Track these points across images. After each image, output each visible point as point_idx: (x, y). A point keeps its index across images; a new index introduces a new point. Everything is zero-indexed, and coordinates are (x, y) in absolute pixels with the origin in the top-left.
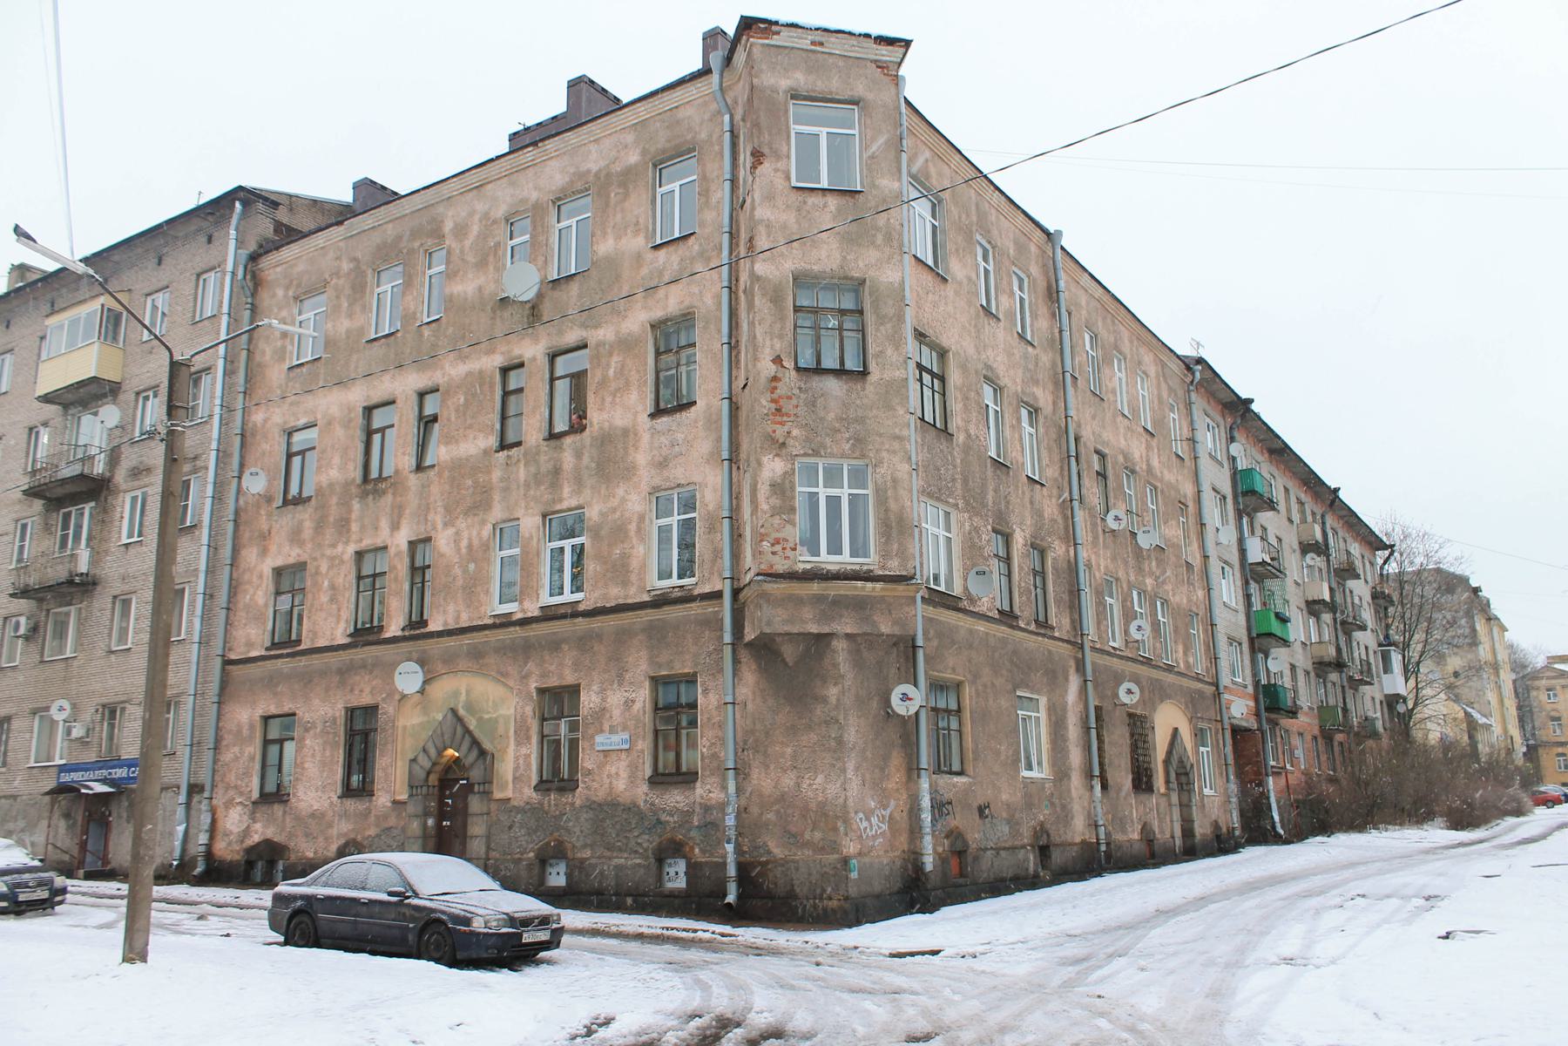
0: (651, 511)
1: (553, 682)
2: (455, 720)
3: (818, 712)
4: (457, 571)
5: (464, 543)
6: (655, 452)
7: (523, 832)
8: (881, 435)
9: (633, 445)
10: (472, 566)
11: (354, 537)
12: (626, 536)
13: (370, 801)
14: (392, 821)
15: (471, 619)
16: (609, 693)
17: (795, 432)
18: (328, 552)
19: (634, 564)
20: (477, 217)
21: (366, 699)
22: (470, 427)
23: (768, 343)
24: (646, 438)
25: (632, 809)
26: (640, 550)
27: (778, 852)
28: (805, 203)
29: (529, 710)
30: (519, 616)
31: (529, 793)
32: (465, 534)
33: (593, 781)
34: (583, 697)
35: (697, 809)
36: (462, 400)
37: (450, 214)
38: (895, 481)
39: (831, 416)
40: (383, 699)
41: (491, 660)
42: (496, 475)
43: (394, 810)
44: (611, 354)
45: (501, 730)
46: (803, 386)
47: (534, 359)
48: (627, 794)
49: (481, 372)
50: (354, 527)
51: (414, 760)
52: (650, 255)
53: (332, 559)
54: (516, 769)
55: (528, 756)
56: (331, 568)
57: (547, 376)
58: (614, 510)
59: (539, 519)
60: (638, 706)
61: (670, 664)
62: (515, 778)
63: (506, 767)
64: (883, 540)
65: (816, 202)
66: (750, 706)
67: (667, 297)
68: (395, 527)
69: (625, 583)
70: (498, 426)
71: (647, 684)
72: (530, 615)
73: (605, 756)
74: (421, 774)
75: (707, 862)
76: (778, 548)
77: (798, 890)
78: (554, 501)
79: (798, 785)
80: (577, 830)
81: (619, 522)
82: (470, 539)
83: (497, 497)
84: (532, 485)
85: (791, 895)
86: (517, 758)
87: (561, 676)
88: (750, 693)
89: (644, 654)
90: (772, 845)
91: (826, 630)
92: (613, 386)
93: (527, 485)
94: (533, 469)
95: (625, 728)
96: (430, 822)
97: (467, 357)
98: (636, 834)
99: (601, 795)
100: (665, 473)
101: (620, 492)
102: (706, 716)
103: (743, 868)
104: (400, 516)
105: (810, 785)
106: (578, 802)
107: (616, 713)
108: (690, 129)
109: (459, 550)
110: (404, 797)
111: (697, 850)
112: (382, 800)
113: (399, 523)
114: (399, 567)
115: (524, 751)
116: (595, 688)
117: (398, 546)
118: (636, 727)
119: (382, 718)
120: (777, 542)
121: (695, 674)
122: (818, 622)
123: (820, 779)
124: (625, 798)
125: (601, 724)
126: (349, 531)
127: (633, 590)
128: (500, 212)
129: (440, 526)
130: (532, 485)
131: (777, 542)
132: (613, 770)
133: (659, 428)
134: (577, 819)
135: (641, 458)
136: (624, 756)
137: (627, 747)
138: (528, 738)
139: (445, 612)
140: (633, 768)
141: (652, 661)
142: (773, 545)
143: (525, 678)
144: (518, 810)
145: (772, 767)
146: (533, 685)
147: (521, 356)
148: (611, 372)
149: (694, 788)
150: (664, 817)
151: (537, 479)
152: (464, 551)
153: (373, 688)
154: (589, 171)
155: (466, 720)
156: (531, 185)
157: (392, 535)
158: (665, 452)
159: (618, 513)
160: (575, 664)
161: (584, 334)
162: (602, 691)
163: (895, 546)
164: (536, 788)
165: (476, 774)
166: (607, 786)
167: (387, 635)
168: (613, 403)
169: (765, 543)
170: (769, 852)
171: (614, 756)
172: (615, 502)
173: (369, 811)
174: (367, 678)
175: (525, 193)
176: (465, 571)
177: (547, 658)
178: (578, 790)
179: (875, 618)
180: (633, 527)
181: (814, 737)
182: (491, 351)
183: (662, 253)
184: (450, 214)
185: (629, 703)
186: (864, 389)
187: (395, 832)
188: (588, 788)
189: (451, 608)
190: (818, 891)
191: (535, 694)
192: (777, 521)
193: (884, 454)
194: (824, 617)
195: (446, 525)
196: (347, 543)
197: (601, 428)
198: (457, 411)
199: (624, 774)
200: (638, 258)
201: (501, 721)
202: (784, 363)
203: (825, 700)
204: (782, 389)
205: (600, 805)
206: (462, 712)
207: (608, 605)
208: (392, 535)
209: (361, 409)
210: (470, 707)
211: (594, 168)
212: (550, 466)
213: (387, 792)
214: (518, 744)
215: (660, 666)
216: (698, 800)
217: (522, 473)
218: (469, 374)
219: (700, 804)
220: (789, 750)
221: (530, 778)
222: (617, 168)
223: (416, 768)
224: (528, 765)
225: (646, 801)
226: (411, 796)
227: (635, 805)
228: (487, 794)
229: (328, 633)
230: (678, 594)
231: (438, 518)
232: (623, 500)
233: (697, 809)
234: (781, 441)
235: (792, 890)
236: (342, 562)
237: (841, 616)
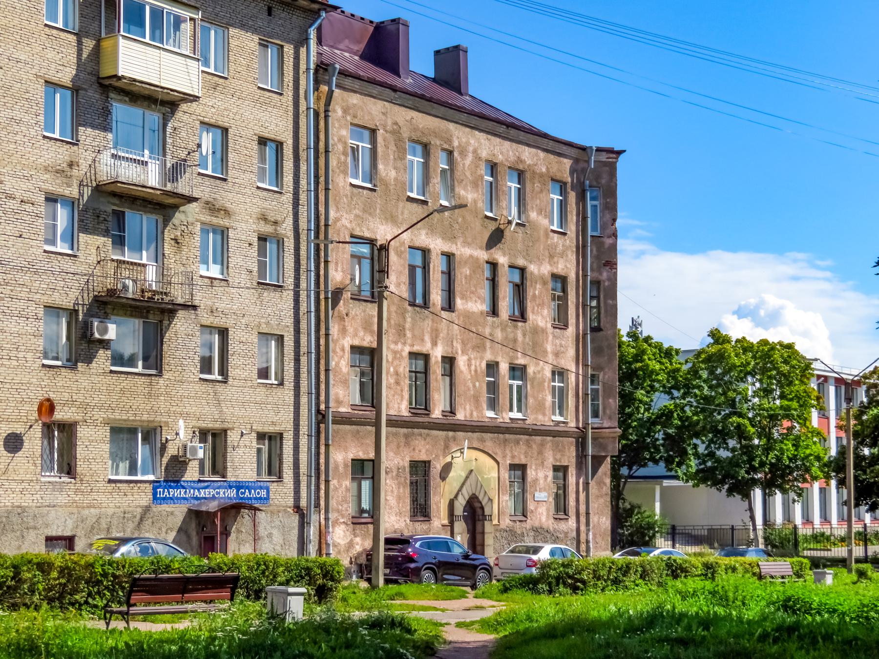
1: (517, 461)
5: (473, 368)
11: (409, 341)
21: (423, 457)
43: (443, 529)
58: (539, 372)
68: (434, 344)
87: (520, 459)
89: (551, 452)
95: (545, 490)
99: (537, 524)
106: (528, 527)
113: (436, 342)
117: (436, 357)
124: (545, 526)
126: (405, 335)
129: (460, 352)
136: (544, 503)
146: (508, 462)
152: (473, 372)
157: (432, 349)
158: (558, 348)
176: (474, 386)
185: (546, 477)
199: (545, 513)
201: (492, 479)
208: (432, 349)
218: (471, 256)
229: (396, 406)
231: (458, 346)
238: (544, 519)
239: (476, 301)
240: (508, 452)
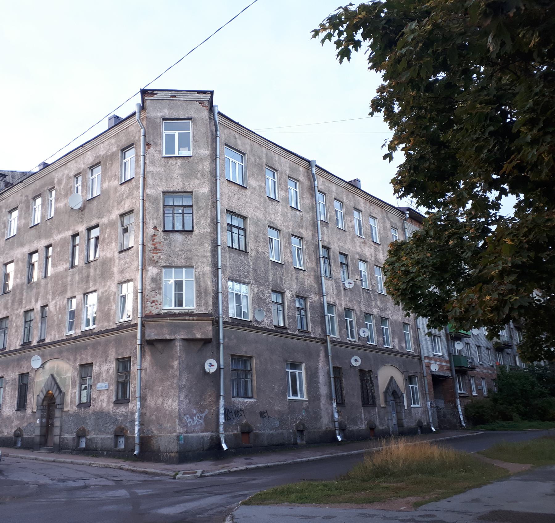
0: (118, 291)
1: (84, 362)
2: (52, 379)
3: (170, 372)
4: (55, 318)
5: (58, 307)
6: (120, 267)
7: (72, 424)
8: (198, 256)
9: (113, 265)
10: (60, 316)
11: (24, 306)
12: (110, 302)
13: (25, 412)
14: (32, 420)
15: (59, 337)
16: (102, 366)
17: (162, 257)
18: (16, 312)
19: (112, 312)
20: (65, 176)
21: (25, 371)
22: (61, 260)
23: (151, 221)
24: (117, 261)
25: (107, 414)
26: (114, 307)
27: (156, 432)
28: (168, 163)
29: (76, 374)
30: (74, 335)
31: (75, 408)
32: (58, 303)
33: (96, 403)
34: (94, 368)
35: (129, 415)
36: (59, 249)
37: (56, 175)
38: (204, 275)
39: (177, 249)
40: (31, 371)
41: (65, 354)
42: (69, 278)
44: (106, 228)
45: (67, 383)
46: (166, 238)
47: (82, 232)
48: (107, 408)
49: (65, 238)
50: (24, 302)
51: (38, 395)
52: (119, 188)
53: (17, 315)
54: (71, 398)
55: (75, 393)
56: (16, 319)
57: (86, 238)
58: (106, 291)
59: (82, 296)
60: (111, 371)
61: (122, 354)
62: (71, 402)
63: (68, 398)
64: (198, 299)
65: (172, 162)
66: (148, 370)
67: (125, 204)
68: (36, 301)
69: (109, 321)
70: (70, 259)
71: (114, 362)
72: (78, 335)
73: (100, 393)
74: (41, 401)
75: (131, 437)
76: (153, 304)
77: (161, 448)
78: (87, 289)
79: (163, 403)
80: (90, 423)
81: (108, 296)
82: (60, 305)
83: (69, 288)
84: (80, 282)
85: (159, 451)
86: (71, 394)
87: (87, 360)
88: (148, 365)
89: (114, 349)
90: (153, 429)
91: (173, 337)
92: (107, 241)
93: (79, 282)
94: (81, 276)
95: (106, 381)
96: (44, 420)
97: (61, 232)
98: (109, 425)
100: (123, 275)
101: (108, 284)
102: (133, 375)
103: (141, 439)
104: (38, 297)
105: (167, 403)
106: (90, 412)
107: (104, 374)
108: (132, 136)
109: (56, 309)
110: (35, 410)
111: (128, 432)
112: (29, 411)
114: (37, 317)
115: (74, 391)
116: (98, 364)
117: (37, 309)
118: (111, 380)
119: (30, 378)
120: (153, 302)
121: (130, 357)
122: (170, 334)
123: (170, 401)
124: (105, 410)
125: (99, 379)
126: (22, 303)
127: (111, 324)
128: (72, 173)
129: (50, 300)
130: (80, 282)
131: (153, 302)
132: (102, 398)
133: (121, 257)
134: (90, 418)
135: (115, 270)
137: (107, 388)
138: (75, 386)
139: (51, 335)
140: (109, 397)
141: (117, 353)
142: (152, 303)
143: (75, 360)
144: (71, 415)
145: (154, 396)
146: (78, 364)
147: (78, 231)
148: (106, 235)
149: (128, 405)
150: (118, 418)
151: (81, 280)
152: (58, 310)
153: (27, 366)
154: (100, 155)
155: (56, 378)
156: (82, 162)
157: (35, 304)
158: (123, 266)
159: (107, 292)
160: (92, 354)
161: (98, 221)
162: (100, 365)
163: (203, 301)
164: (78, 406)
165: (58, 401)
166: (100, 405)
167: (32, 345)
168: (107, 248)
169: (148, 303)
170: (152, 432)
171: (102, 392)
172: (106, 288)
173: (24, 415)
174: (25, 362)
175: (80, 166)
176: (58, 318)
177: (83, 352)
178: (91, 407)
179: (194, 332)
180: (112, 298)
181: (169, 383)
182: (68, 230)
183: (123, 186)
184: (56, 175)
185: (108, 370)
186: (191, 237)
187: (32, 424)
188: (94, 406)
189: (53, 333)
190: (168, 449)
191: (78, 367)
192: (153, 293)
193: (199, 264)
194: (172, 332)
195: (52, 300)
196: (21, 308)
197: (103, 258)
198: (57, 254)
199: (106, 400)
200: (116, 189)
201: (67, 379)
202: (158, 229)
203: (172, 367)
204: (157, 240)
205: (97, 413)
206: (55, 375)
207: (103, 330)
208: (35, 304)
209: (27, 255)
210: (58, 374)
211: (102, 154)
212: (86, 274)
213: (31, 408)
214: (72, 388)
215: (119, 355)
216: (129, 410)
217: (77, 278)
218: (61, 239)
219: (130, 412)
220: (160, 389)
221: (75, 402)
222: (109, 153)
223: (39, 398)
224: (75, 397)
225: (112, 411)
226: (37, 410)
227: (109, 413)
228: (62, 409)
229: (14, 344)
230: (126, 324)
231: (50, 297)
232: (109, 287)
233: (129, 415)
234: (156, 261)
235: (159, 448)
236: (20, 316)
237: (180, 332)
238: (104, 405)
239: (62, 264)
240: (78, 357)
